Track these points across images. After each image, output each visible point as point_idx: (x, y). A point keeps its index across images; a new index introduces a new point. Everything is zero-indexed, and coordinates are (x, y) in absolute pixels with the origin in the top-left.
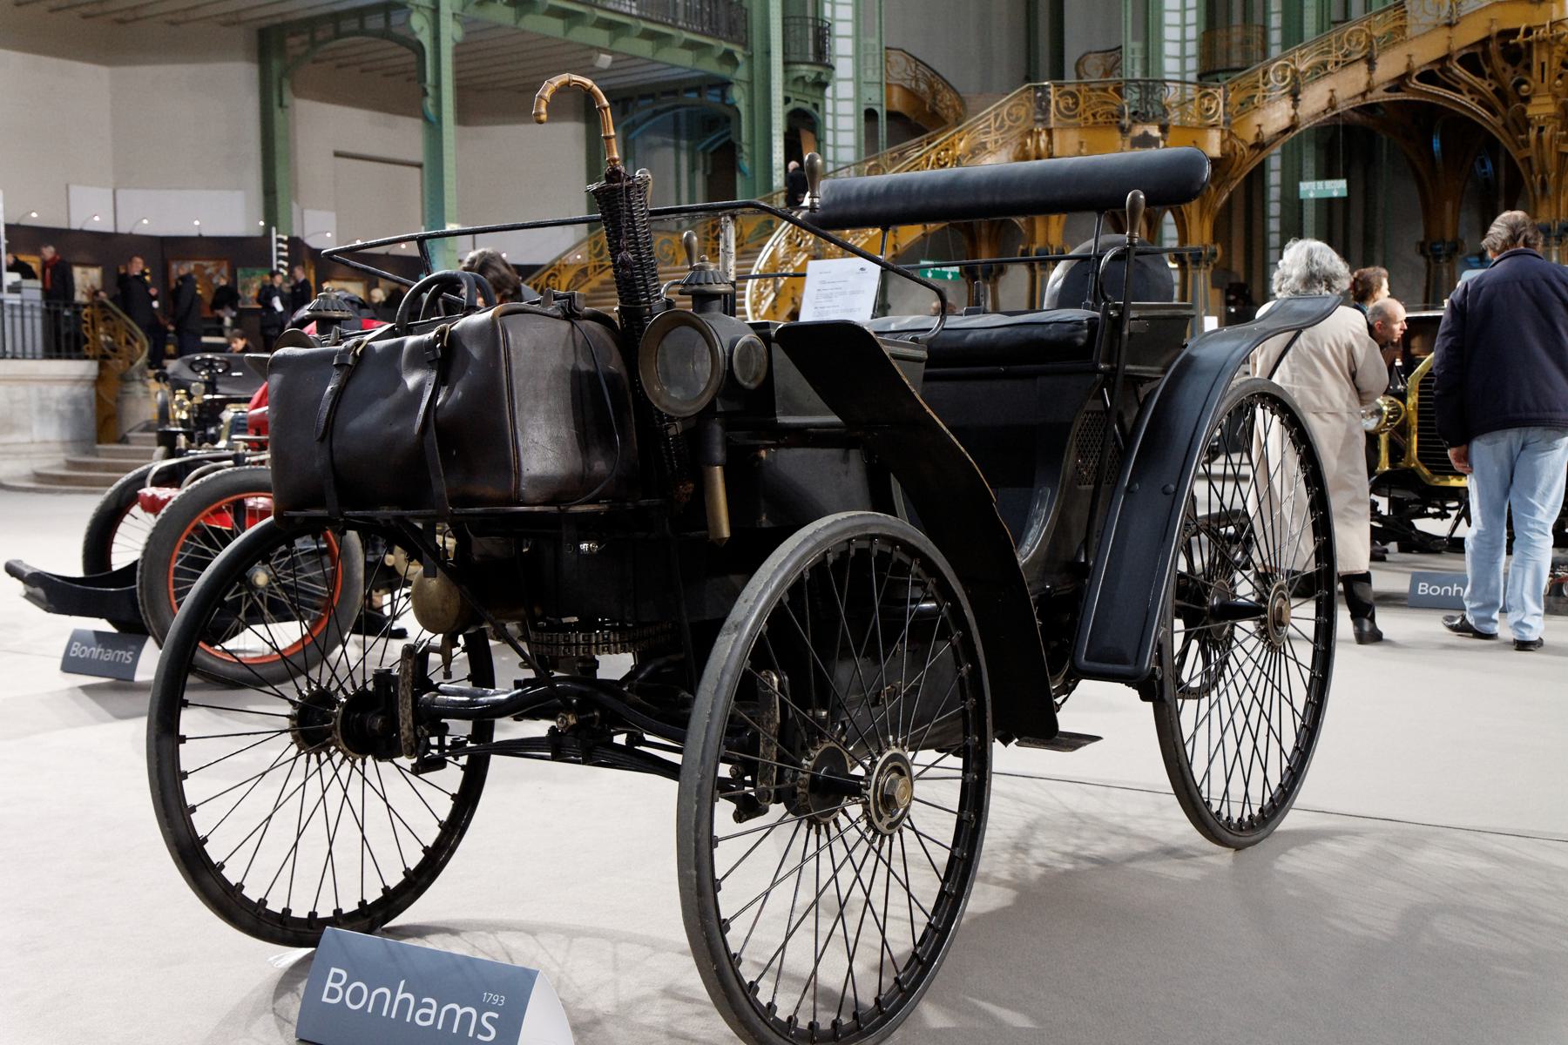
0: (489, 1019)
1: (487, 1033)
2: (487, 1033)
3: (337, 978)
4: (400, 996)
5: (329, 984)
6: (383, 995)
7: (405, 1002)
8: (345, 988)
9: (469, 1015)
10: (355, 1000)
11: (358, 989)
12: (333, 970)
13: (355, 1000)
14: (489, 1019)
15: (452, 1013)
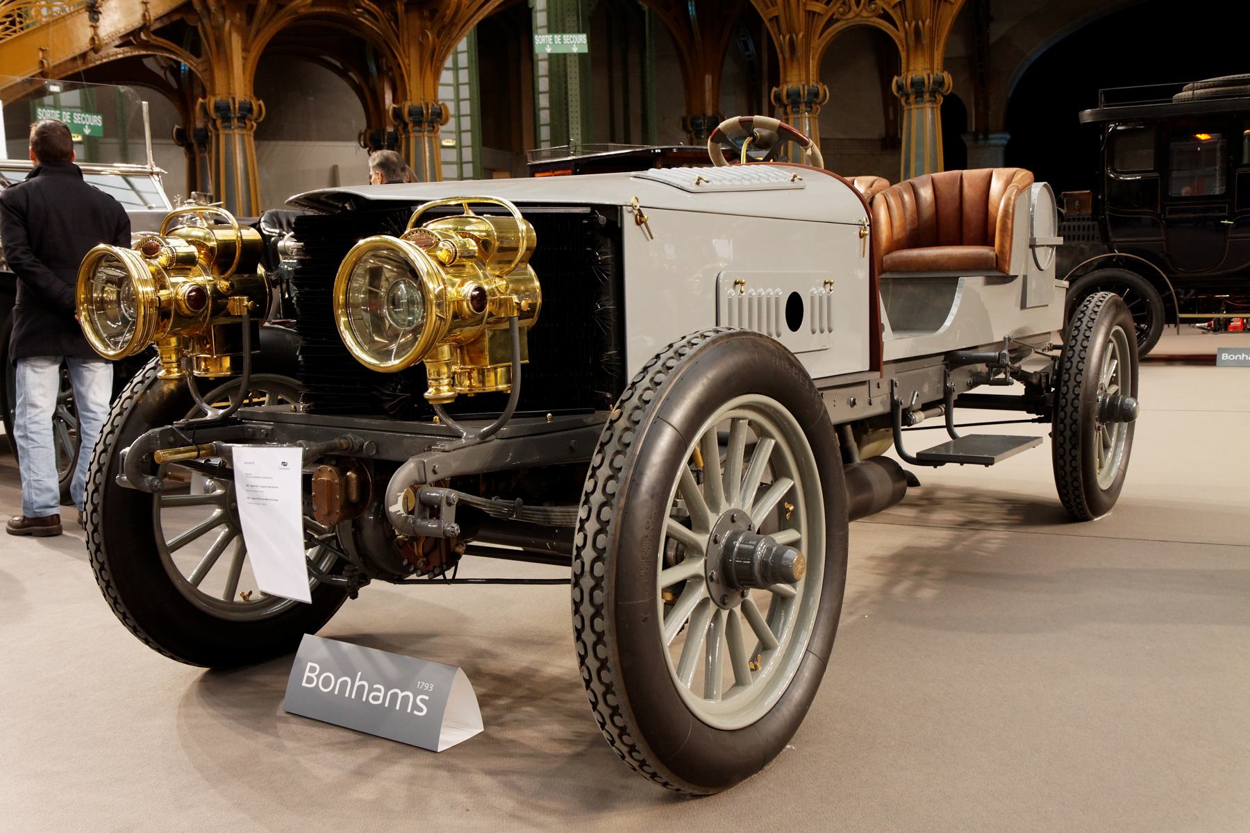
0: (422, 700)
1: (421, 710)
2: (421, 710)
3: (312, 670)
4: (357, 683)
5: (307, 674)
6: (344, 684)
7: (361, 688)
8: (318, 677)
9: (407, 697)
10: (326, 686)
11: (328, 678)
12: (310, 664)
13: (326, 686)
14: (422, 700)
15: (395, 696)
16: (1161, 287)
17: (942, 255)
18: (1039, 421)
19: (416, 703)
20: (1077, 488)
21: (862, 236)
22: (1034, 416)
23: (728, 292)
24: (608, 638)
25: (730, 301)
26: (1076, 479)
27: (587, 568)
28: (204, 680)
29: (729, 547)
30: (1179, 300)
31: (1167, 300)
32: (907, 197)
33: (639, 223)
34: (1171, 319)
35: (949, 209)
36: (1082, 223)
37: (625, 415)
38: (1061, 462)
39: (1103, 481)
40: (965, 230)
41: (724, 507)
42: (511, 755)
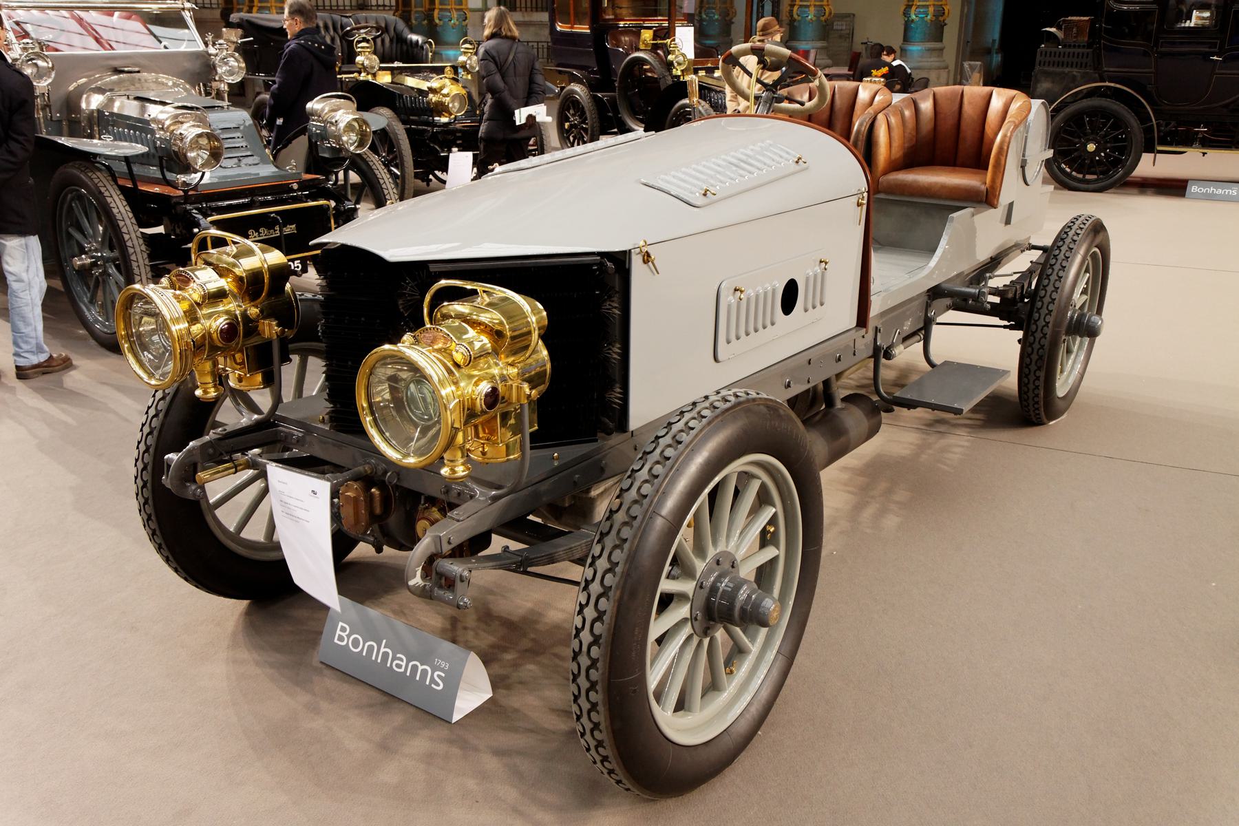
4: (383, 650)
7: (386, 655)
11: (356, 647)
16: (1143, 118)
17: (936, 183)
18: (1011, 327)
19: (436, 679)
20: (1037, 403)
21: (859, 205)
22: (1006, 323)
23: (728, 299)
24: (600, 708)
25: (729, 306)
26: (1037, 396)
27: (585, 648)
28: (248, 613)
29: (714, 589)
30: (1159, 131)
31: (1148, 131)
32: (907, 113)
33: (646, 262)
34: (1150, 149)
35: (949, 123)
36: (1077, 50)
37: (624, 508)
38: (1026, 371)
39: (1061, 389)
40: (960, 147)
41: (711, 552)
42: (515, 730)
